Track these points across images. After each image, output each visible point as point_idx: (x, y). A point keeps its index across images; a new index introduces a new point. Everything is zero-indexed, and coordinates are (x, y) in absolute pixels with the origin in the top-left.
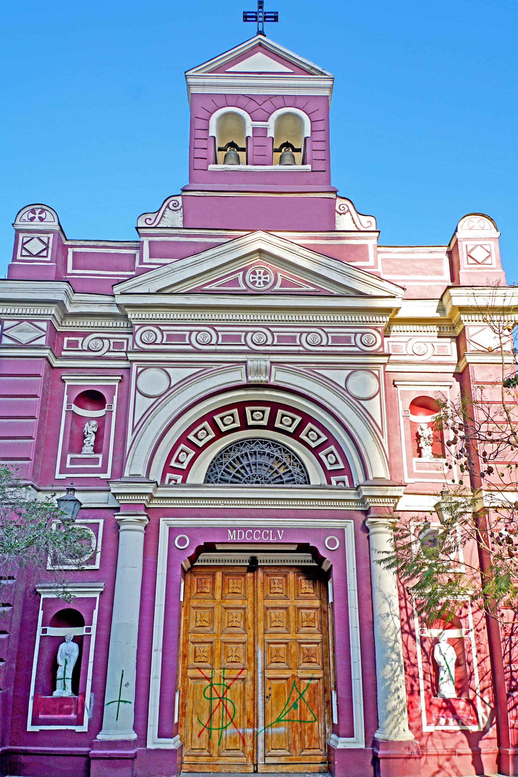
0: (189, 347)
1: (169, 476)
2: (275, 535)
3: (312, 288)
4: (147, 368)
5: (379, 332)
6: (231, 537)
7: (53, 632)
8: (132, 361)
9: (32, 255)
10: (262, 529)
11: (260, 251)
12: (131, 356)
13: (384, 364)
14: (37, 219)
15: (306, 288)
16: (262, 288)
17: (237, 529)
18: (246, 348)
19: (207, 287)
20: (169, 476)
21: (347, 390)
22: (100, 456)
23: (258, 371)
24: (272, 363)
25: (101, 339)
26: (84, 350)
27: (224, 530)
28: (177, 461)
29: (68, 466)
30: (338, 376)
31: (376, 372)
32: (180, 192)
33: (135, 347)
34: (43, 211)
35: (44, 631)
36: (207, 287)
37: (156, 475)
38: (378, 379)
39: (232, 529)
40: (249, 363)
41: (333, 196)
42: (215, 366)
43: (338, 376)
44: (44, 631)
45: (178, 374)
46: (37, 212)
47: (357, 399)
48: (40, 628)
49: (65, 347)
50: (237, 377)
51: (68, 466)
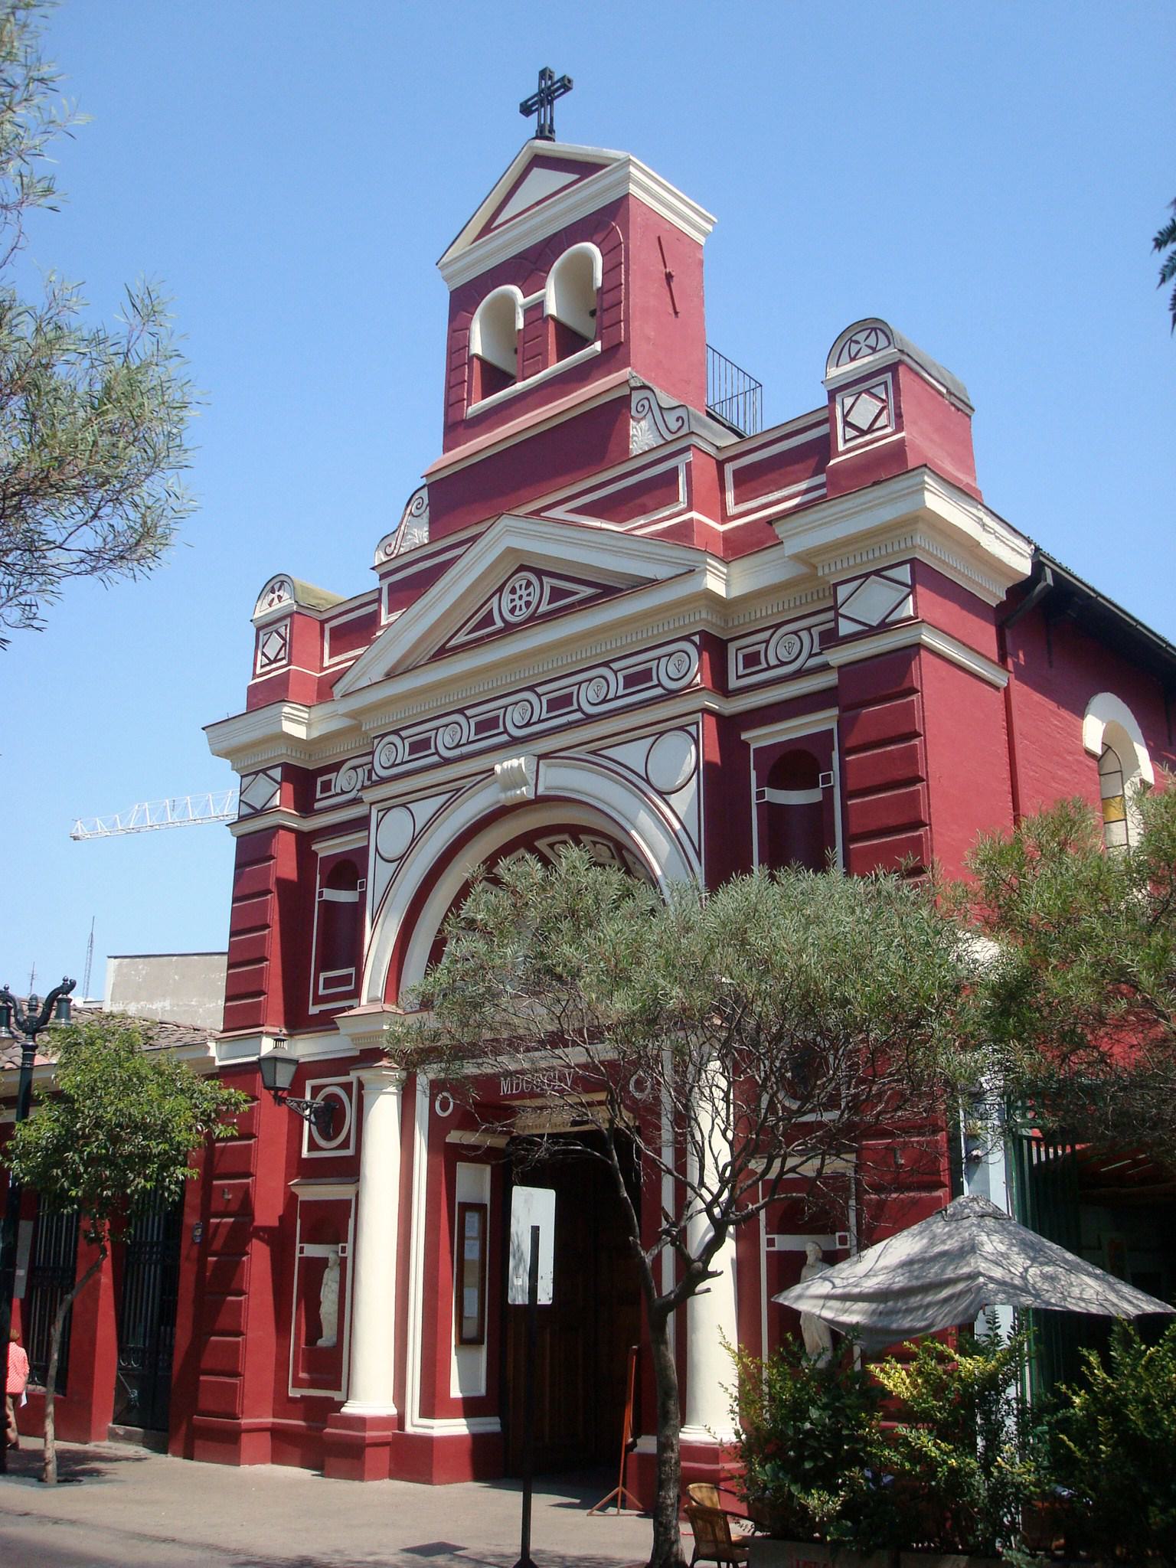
0: (436, 758)
3: (589, 591)
4: (389, 809)
5: (694, 643)
7: (313, 1251)
8: (372, 804)
9: (271, 662)
11: (510, 551)
12: (369, 796)
14: (276, 600)
16: (522, 615)
19: (453, 643)
22: (352, 970)
24: (541, 757)
25: (354, 768)
26: (337, 794)
29: (321, 992)
31: (692, 729)
32: (424, 481)
33: (374, 777)
34: (282, 582)
35: (302, 1250)
36: (453, 643)
40: (498, 768)
43: (631, 754)
44: (302, 1249)
45: (424, 810)
46: (276, 587)
48: (298, 1246)
49: (318, 796)
51: (321, 992)
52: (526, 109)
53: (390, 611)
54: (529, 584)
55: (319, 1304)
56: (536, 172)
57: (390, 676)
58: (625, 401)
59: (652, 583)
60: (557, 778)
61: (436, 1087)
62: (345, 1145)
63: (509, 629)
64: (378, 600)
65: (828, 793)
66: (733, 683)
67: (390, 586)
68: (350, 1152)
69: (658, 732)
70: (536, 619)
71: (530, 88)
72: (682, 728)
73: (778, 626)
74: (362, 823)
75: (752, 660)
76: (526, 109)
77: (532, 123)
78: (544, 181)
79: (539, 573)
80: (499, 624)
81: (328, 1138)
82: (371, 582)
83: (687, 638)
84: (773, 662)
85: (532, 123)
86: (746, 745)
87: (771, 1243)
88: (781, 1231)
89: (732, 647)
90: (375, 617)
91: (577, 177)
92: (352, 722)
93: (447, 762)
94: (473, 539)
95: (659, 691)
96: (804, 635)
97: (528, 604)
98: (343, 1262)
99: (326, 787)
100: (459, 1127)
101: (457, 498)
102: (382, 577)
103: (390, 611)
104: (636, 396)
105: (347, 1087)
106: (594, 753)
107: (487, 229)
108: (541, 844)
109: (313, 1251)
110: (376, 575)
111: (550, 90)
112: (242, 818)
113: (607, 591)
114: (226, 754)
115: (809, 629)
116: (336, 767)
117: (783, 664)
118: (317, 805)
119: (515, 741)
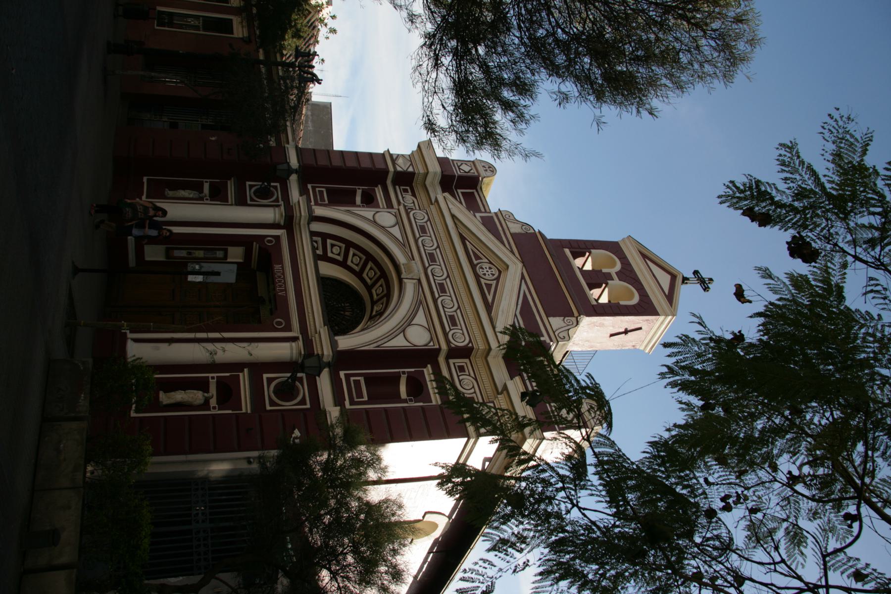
1: (319, 239)
2: (282, 291)
6: (277, 267)
7: (206, 187)
10: (285, 283)
12: (402, 208)
13: (439, 350)
15: (490, 298)
17: (283, 269)
18: (427, 265)
20: (319, 239)
21: (409, 325)
23: (409, 269)
27: (281, 261)
28: (333, 246)
30: (420, 318)
31: (431, 344)
37: (316, 227)
38: (426, 345)
39: (283, 267)
41: (576, 313)
42: (408, 250)
43: (420, 318)
45: (396, 231)
47: (404, 331)
50: (401, 258)
52: (696, 273)
53: (481, 217)
54: (493, 275)
55: (184, 189)
56: (668, 277)
57: (453, 217)
58: (572, 315)
59: (494, 328)
60: (410, 288)
61: (277, 238)
62: (252, 200)
63: (473, 267)
64: (486, 212)
65: (405, 401)
66: (451, 361)
67: (492, 217)
68: (249, 202)
69: (431, 329)
70: (477, 277)
71: (705, 275)
72: (432, 339)
73: (476, 379)
74: (390, 205)
75: (462, 369)
76: (696, 273)
77: (690, 275)
78: (665, 280)
79: (498, 279)
80: (475, 262)
81: (255, 193)
82: (494, 209)
83: (470, 341)
84: (461, 378)
85: (690, 275)
86: (425, 367)
87: (213, 378)
88: (218, 382)
89: (467, 361)
90: (480, 211)
91: (667, 292)
92: (433, 200)
93: (416, 241)
94: (512, 252)
95: (448, 329)
96: (472, 391)
97: (485, 274)
98: (201, 199)
99: (406, 191)
100: (260, 247)
101: (529, 244)
102: (496, 214)
103: (481, 217)
104: (574, 319)
105: (277, 200)
106: (421, 302)
107: (645, 256)
108: (382, 281)
109: (206, 187)
110: (496, 210)
111: (705, 283)
112: (391, 155)
113: (489, 307)
114: (419, 146)
115: (475, 392)
116: (414, 195)
117: (460, 381)
118: (397, 187)
119: (425, 270)
